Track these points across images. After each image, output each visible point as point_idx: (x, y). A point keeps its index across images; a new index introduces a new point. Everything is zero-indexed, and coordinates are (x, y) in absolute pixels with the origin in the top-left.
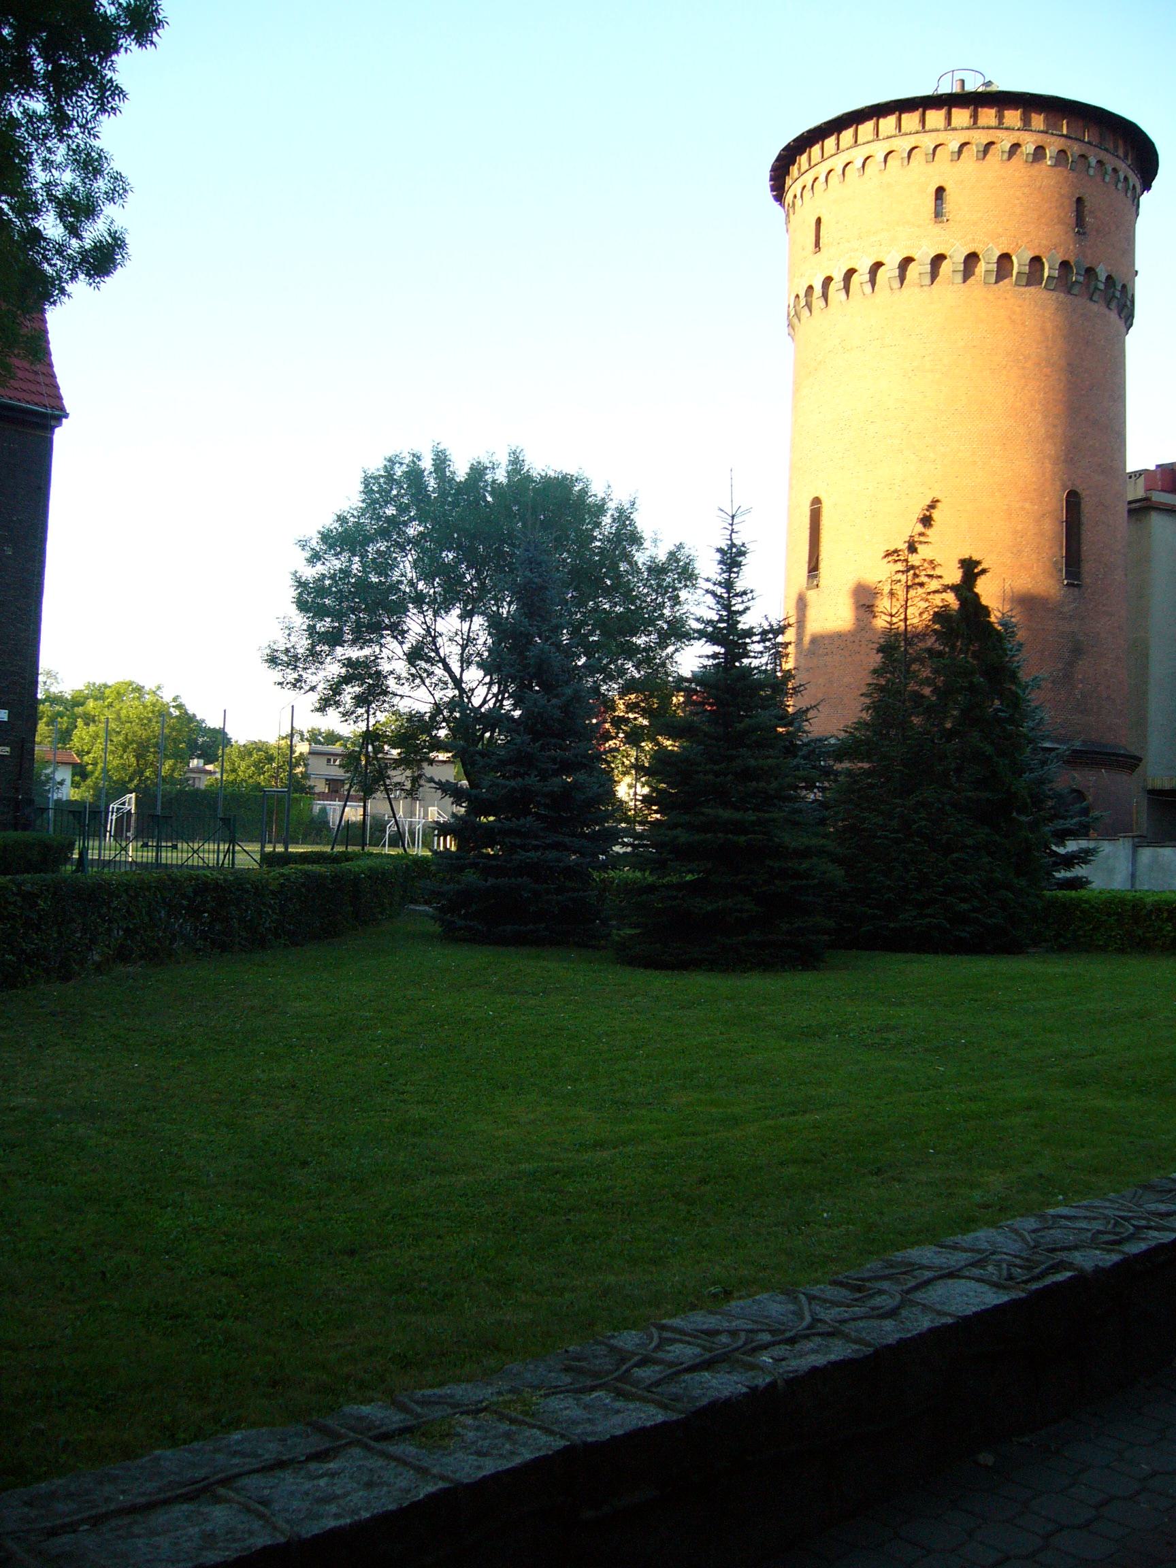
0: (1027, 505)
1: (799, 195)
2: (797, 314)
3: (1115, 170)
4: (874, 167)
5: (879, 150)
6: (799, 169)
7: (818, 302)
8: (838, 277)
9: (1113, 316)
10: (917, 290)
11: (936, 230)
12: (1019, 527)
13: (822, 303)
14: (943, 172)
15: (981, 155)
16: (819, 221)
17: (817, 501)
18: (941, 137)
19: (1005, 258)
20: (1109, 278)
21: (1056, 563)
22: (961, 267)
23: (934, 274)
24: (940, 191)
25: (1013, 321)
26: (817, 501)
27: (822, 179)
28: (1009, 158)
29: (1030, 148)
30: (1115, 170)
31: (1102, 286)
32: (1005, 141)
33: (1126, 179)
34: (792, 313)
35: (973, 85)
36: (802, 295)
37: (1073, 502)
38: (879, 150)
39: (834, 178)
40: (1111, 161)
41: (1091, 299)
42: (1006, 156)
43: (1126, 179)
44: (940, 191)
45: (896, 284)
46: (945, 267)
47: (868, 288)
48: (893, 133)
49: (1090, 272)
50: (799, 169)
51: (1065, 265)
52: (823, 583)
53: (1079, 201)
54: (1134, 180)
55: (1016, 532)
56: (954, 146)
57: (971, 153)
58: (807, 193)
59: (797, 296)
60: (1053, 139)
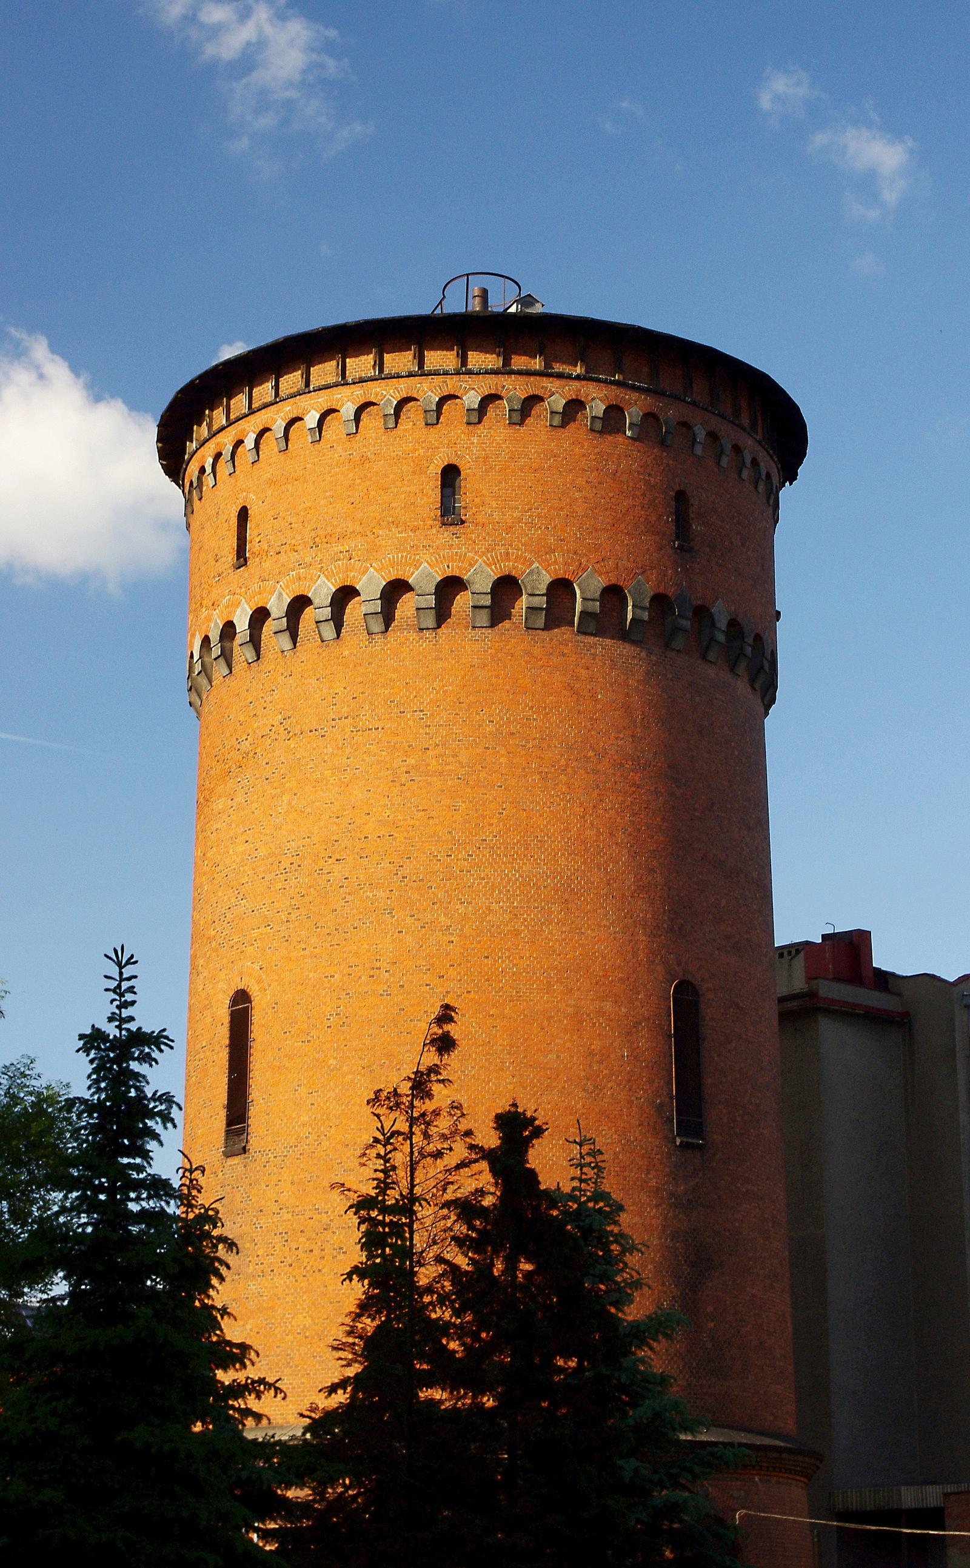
0: (608, 1006)
1: (208, 469)
2: (205, 671)
3: (737, 449)
4: (335, 429)
5: (347, 401)
6: (210, 426)
7: (242, 653)
8: (278, 606)
9: (742, 686)
10: (413, 636)
11: (444, 536)
12: (596, 1045)
13: (250, 654)
14: (454, 441)
15: (516, 417)
16: (243, 515)
17: (241, 998)
18: (451, 385)
19: (561, 588)
20: (733, 623)
21: (660, 1108)
22: (487, 601)
24: (450, 475)
25: (575, 693)
26: (241, 998)
27: (249, 442)
28: (564, 425)
29: (598, 408)
30: (737, 449)
31: (721, 638)
32: (557, 397)
33: (755, 463)
34: (198, 668)
35: (504, 301)
36: (214, 637)
37: (687, 1001)
38: (347, 401)
39: (270, 445)
40: (729, 435)
41: (704, 657)
42: (557, 420)
44: (450, 475)
45: (377, 625)
46: (462, 602)
47: (329, 631)
48: (371, 373)
49: (702, 613)
50: (210, 426)
51: (659, 600)
52: (254, 1143)
53: (681, 497)
55: (592, 1053)
56: (472, 399)
57: (498, 412)
58: (224, 468)
59: (206, 640)
60: (634, 396)
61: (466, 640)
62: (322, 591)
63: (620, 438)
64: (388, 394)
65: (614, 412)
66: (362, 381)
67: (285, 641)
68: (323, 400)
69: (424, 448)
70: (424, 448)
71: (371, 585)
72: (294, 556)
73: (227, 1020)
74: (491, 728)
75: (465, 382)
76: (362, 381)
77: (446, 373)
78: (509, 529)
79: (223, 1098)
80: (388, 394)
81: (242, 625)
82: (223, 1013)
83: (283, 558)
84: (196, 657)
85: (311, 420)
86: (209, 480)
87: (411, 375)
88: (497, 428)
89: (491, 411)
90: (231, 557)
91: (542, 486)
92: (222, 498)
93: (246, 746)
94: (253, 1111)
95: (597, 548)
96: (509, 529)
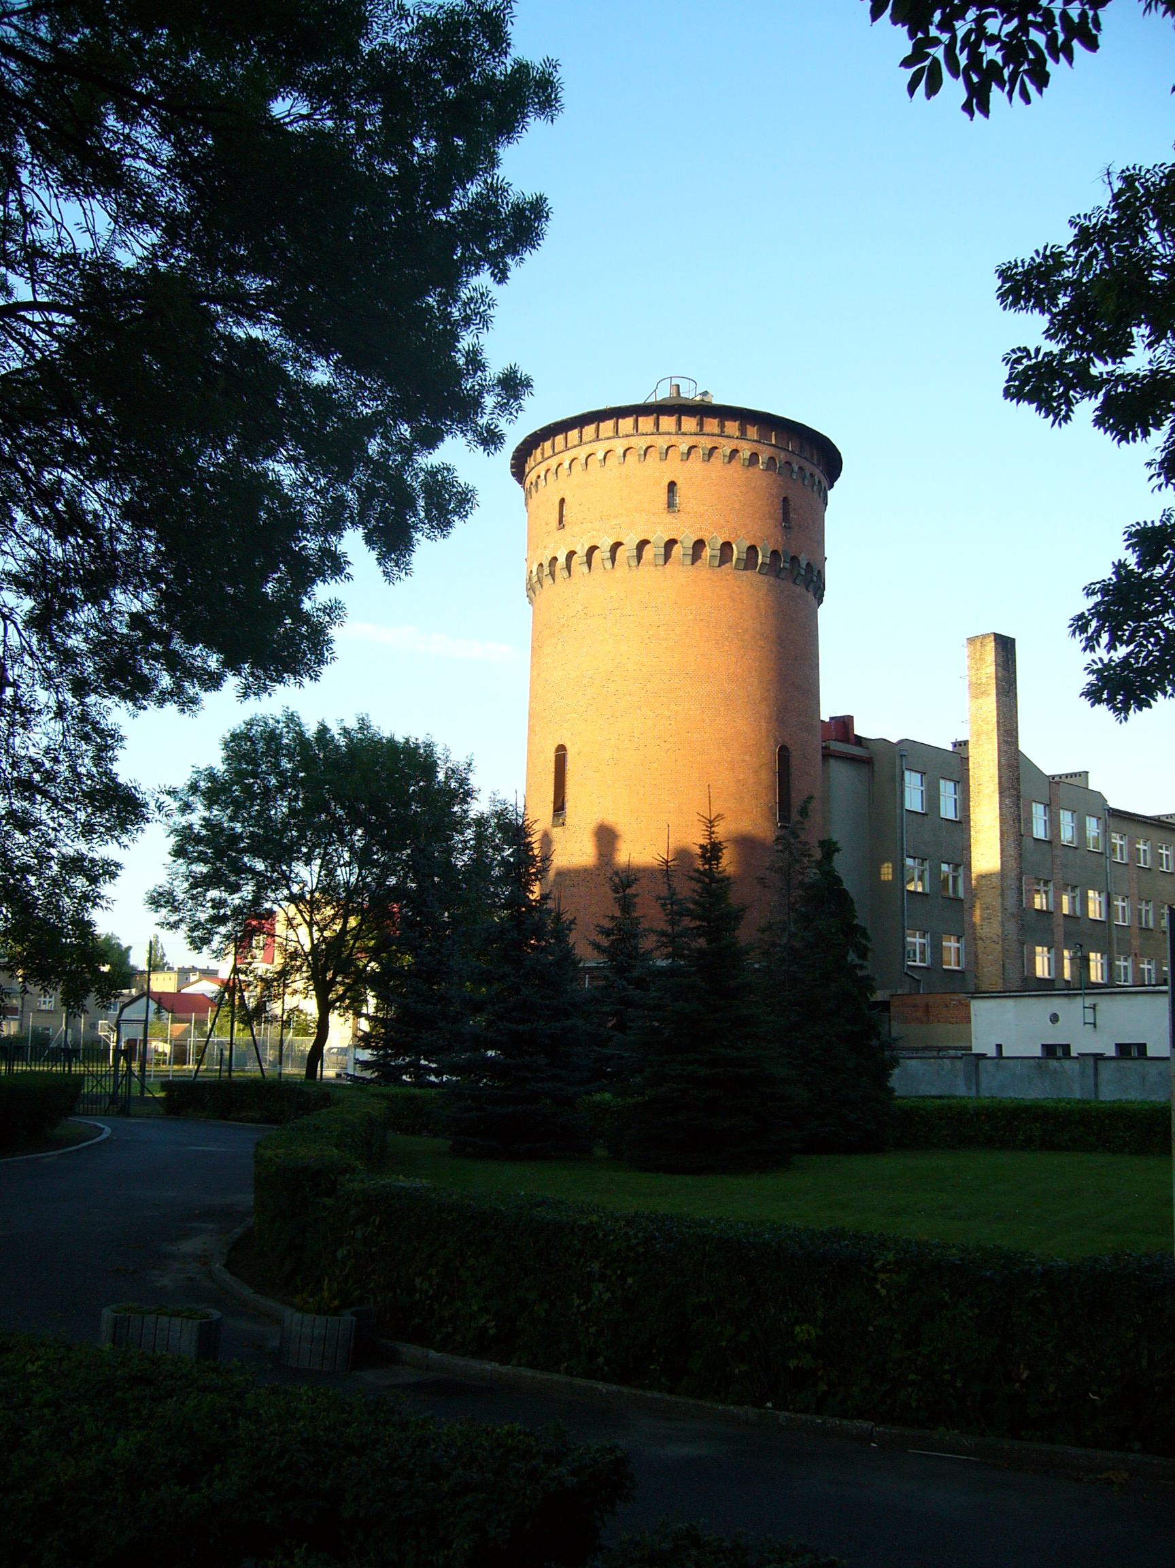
0: (747, 758)
1: (542, 477)
2: (540, 581)
3: (812, 475)
4: (612, 461)
5: (619, 446)
6: (543, 454)
7: (560, 573)
8: (581, 552)
9: (810, 596)
10: (652, 568)
11: (669, 518)
12: (741, 777)
13: (566, 574)
14: (674, 469)
15: (706, 458)
16: (562, 501)
17: (561, 748)
18: (674, 439)
19: (727, 546)
20: (808, 564)
21: (771, 808)
22: (691, 552)
23: (667, 556)
24: (672, 485)
25: (734, 601)
26: (561, 748)
27: (566, 465)
28: (730, 462)
29: (747, 454)
30: (812, 475)
31: (803, 572)
32: (726, 447)
33: (819, 482)
34: (535, 579)
35: (689, 393)
36: (546, 564)
37: (784, 756)
38: (619, 446)
39: (577, 467)
40: (809, 468)
41: (794, 582)
42: (727, 459)
43: (819, 482)
44: (672, 485)
45: (634, 563)
46: (677, 550)
47: (608, 564)
48: (632, 432)
49: (794, 560)
50: (543, 454)
51: (775, 553)
52: (568, 821)
53: (785, 500)
54: (819, 475)
55: (739, 781)
56: (684, 448)
57: (697, 455)
58: (550, 476)
59: (541, 565)
60: (765, 448)
61: (679, 572)
62: (606, 544)
63: (756, 470)
64: (641, 443)
65: (754, 456)
66: (627, 436)
67: (585, 568)
68: (606, 445)
69: (659, 472)
70: (659, 472)
71: (630, 542)
72: (590, 525)
73: (553, 759)
74: (691, 617)
75: (680, 439)
76: (627, 436)
77: (669, 434)
78: (701, 516)
79: (552, 798)
80: (641, 443)
81: (562, 560)
82: (551, 756)
83: (584, 526)
84: (534, 573)
85: (600, 455)
86: (542, 482)
87: (652, 434)
88: (696, 463)
89: (693, 455)
90: (555, 523)
91: (721, 495)
92: (549, 493)
93: (563, 621)
94: (568, 805)
95: (745, 525)
96: (701, 516)
